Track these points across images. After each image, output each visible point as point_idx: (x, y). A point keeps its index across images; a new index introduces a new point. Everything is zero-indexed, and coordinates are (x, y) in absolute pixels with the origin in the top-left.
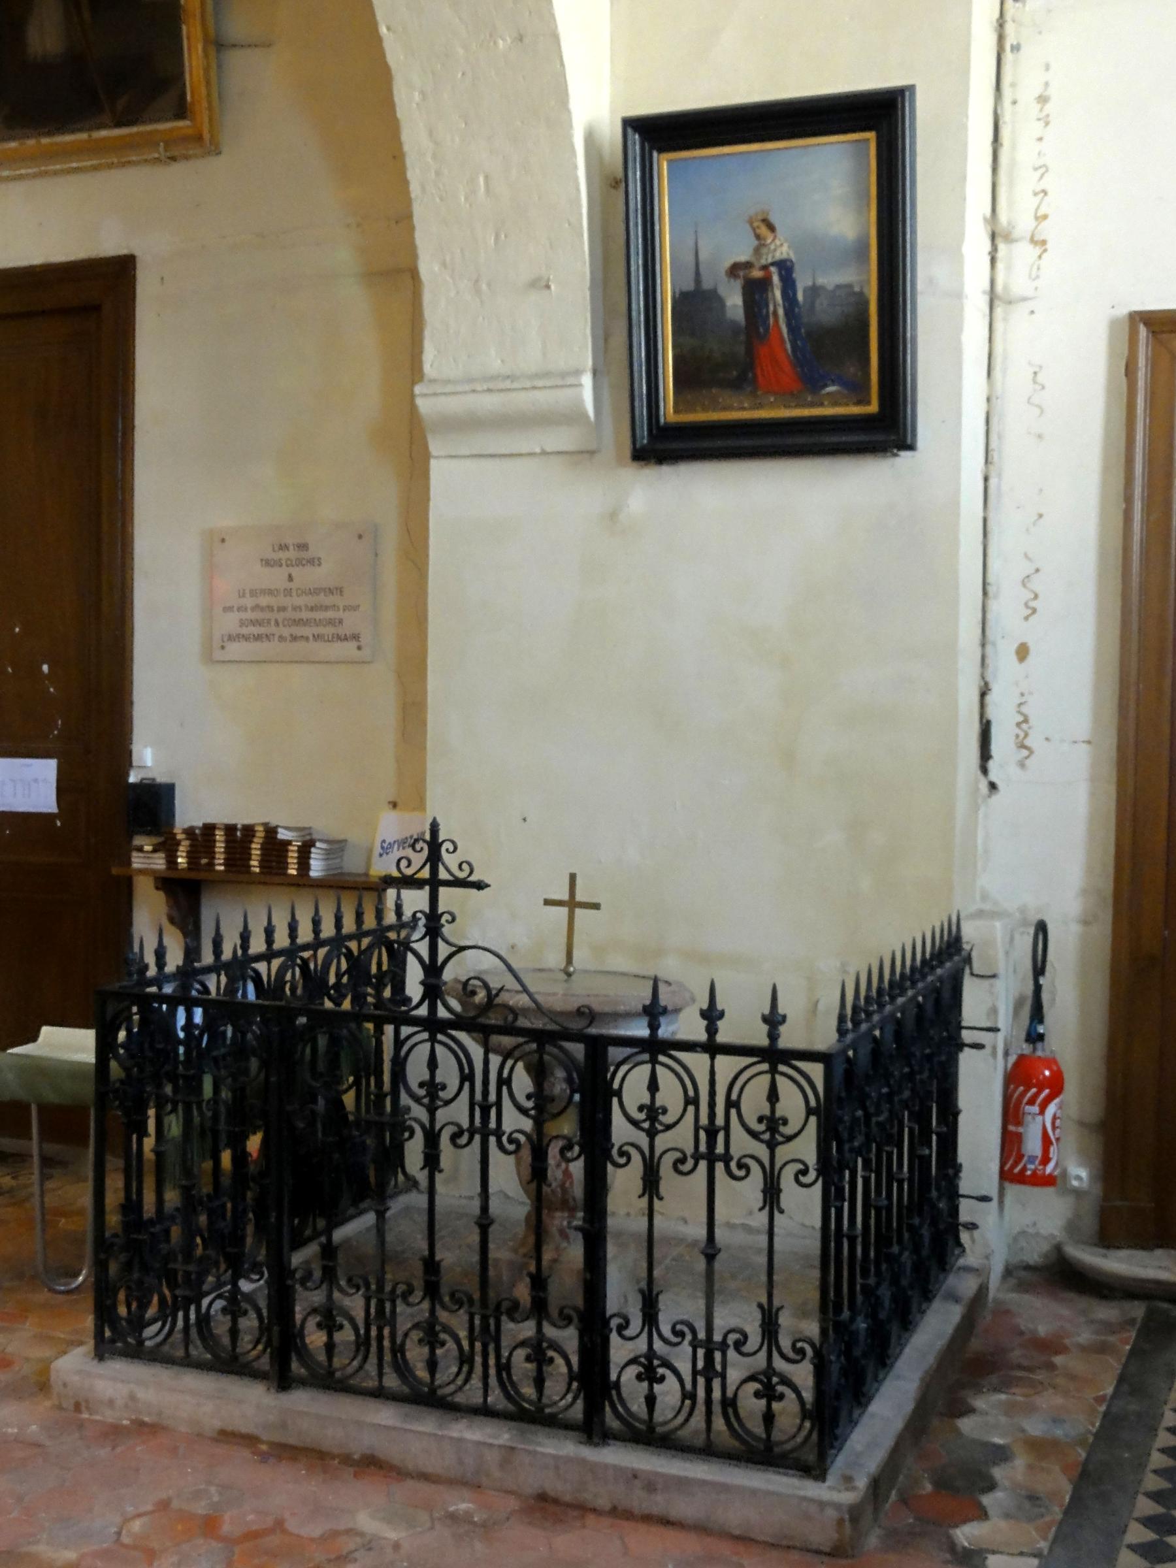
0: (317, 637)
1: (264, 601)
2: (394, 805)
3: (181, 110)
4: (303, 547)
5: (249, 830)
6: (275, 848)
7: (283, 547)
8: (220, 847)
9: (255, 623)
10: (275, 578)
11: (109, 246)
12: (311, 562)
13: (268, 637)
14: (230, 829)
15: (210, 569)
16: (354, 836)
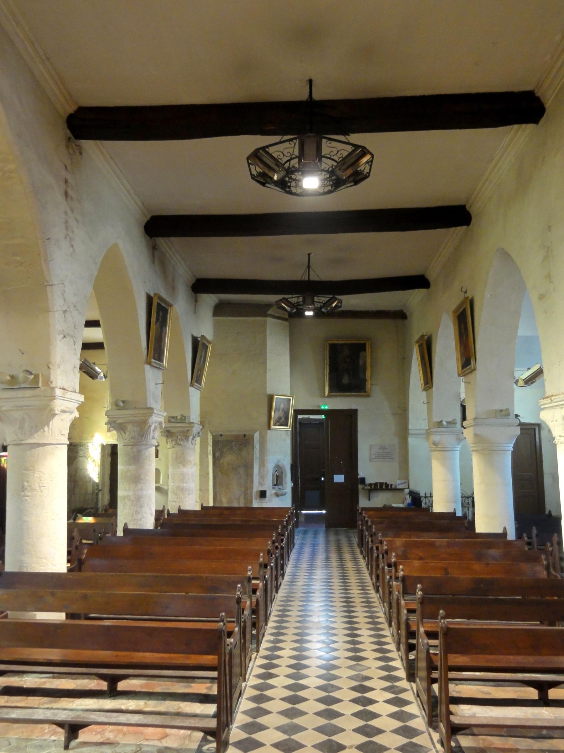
0: (387, 458)
1: (380, 454)
2: (399, 479)
3: (365, 391)
4: (385, 447)
5: (383, 483)
6: (387, 485)
7: (382, 447)
8: (379, 485)
9: (378, 456)
10: (381, 451)
11: (353, 407)
12: (386, 449)
13: (380, 458)
14: (380, 483)
15: (370, 450)
16: (394, 484)
